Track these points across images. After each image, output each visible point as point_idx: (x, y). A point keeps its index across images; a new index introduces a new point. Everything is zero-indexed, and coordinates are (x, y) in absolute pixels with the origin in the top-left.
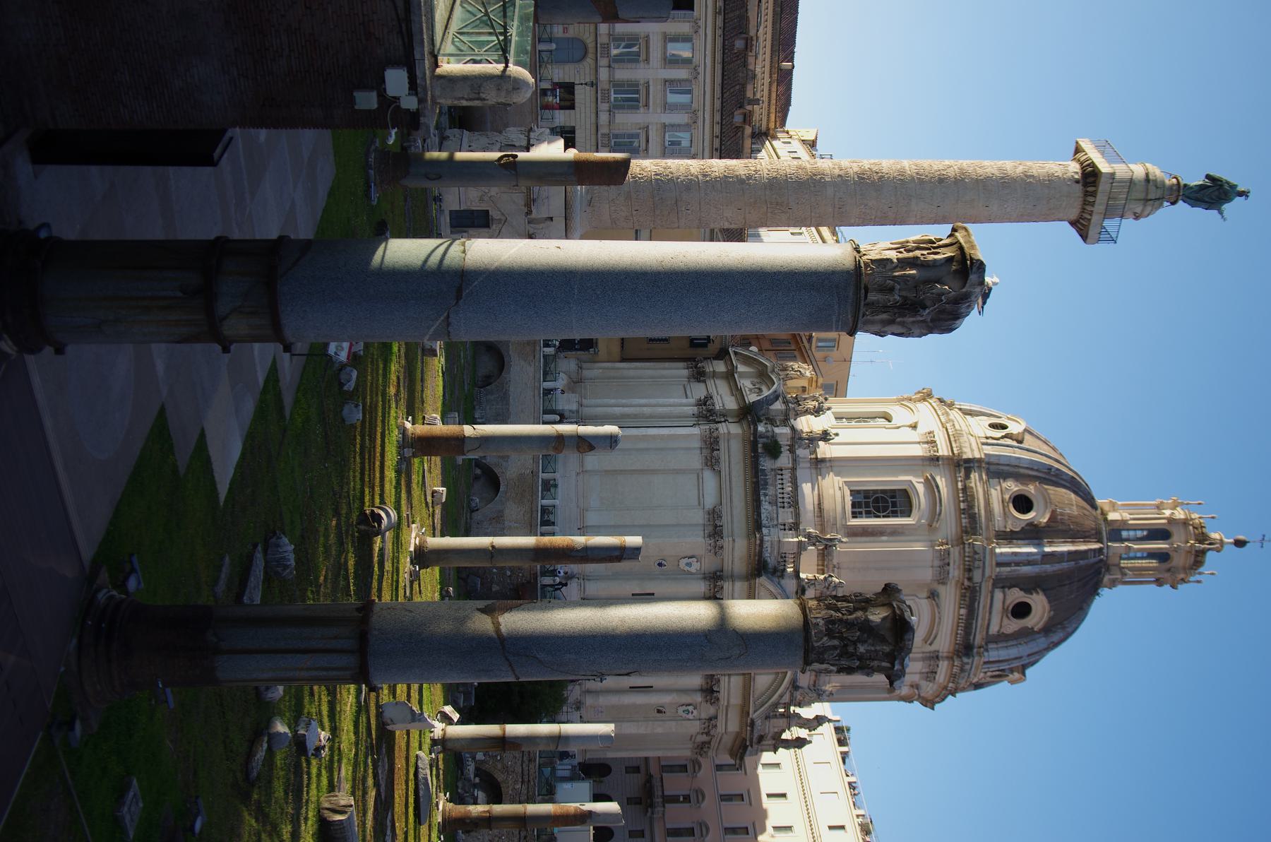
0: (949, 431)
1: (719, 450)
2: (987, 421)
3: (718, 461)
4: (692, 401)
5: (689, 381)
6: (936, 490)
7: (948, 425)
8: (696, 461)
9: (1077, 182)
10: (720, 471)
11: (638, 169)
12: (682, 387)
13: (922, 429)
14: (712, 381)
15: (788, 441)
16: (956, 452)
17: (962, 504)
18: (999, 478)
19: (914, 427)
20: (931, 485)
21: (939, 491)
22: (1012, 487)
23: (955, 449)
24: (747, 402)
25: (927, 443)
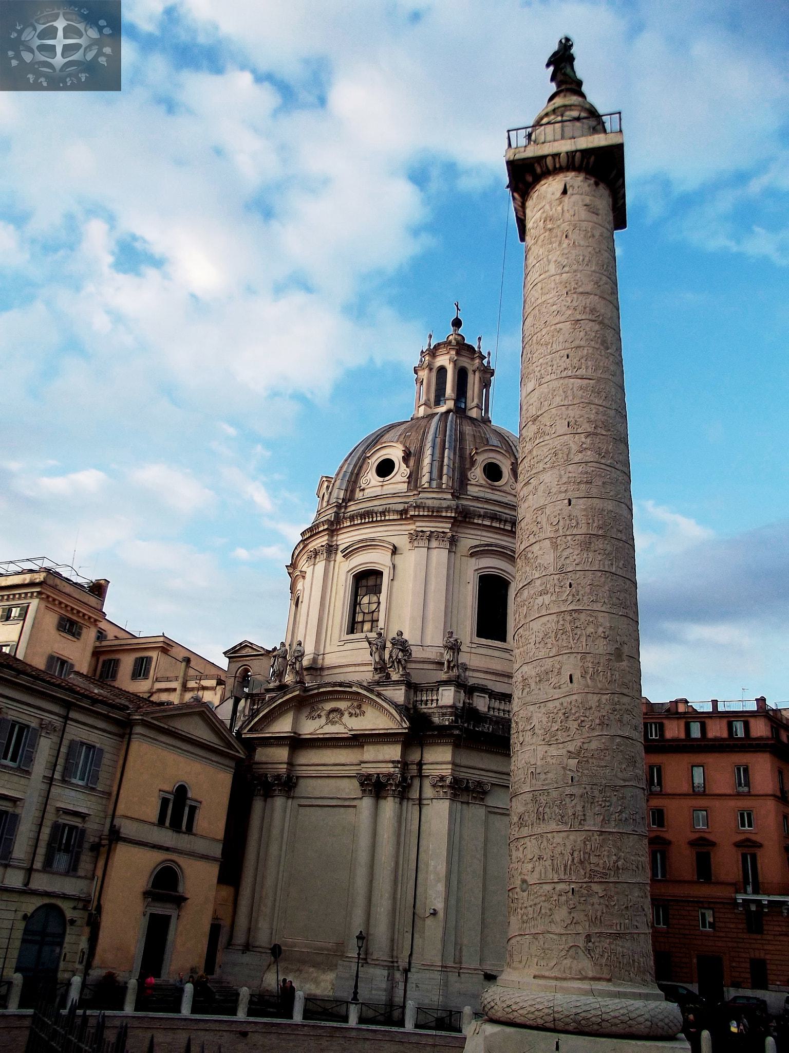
0: (421, 513)
1: (468, 780)
2: (370, 478)
3: (480, 784)
4: (367, 803)
5: (293, 798)
6: (490, 548)
7: (412, 513)
8: (476, 812)
9: (597, 184)
10: (491, 783)
11: (593, 860)
12: (302, 810)
13: (402, 541)
14: (298, 768)
15: (460, 692)
16: (453, 515)
17: (506, 528)
18: (467, 484)
19: (395, 551)
20: (476, 553)
21: (491, 545)
22: (477, 474)
23: (449, 515)
24: (407, 731)
25: (429, 540)
